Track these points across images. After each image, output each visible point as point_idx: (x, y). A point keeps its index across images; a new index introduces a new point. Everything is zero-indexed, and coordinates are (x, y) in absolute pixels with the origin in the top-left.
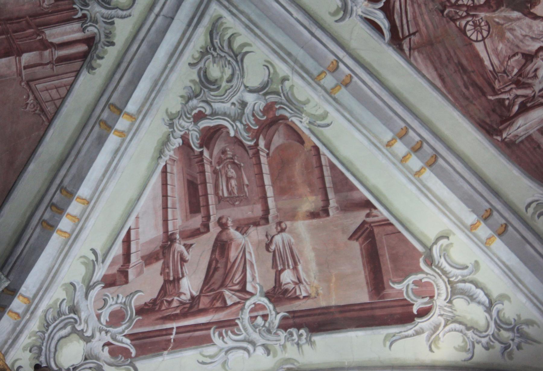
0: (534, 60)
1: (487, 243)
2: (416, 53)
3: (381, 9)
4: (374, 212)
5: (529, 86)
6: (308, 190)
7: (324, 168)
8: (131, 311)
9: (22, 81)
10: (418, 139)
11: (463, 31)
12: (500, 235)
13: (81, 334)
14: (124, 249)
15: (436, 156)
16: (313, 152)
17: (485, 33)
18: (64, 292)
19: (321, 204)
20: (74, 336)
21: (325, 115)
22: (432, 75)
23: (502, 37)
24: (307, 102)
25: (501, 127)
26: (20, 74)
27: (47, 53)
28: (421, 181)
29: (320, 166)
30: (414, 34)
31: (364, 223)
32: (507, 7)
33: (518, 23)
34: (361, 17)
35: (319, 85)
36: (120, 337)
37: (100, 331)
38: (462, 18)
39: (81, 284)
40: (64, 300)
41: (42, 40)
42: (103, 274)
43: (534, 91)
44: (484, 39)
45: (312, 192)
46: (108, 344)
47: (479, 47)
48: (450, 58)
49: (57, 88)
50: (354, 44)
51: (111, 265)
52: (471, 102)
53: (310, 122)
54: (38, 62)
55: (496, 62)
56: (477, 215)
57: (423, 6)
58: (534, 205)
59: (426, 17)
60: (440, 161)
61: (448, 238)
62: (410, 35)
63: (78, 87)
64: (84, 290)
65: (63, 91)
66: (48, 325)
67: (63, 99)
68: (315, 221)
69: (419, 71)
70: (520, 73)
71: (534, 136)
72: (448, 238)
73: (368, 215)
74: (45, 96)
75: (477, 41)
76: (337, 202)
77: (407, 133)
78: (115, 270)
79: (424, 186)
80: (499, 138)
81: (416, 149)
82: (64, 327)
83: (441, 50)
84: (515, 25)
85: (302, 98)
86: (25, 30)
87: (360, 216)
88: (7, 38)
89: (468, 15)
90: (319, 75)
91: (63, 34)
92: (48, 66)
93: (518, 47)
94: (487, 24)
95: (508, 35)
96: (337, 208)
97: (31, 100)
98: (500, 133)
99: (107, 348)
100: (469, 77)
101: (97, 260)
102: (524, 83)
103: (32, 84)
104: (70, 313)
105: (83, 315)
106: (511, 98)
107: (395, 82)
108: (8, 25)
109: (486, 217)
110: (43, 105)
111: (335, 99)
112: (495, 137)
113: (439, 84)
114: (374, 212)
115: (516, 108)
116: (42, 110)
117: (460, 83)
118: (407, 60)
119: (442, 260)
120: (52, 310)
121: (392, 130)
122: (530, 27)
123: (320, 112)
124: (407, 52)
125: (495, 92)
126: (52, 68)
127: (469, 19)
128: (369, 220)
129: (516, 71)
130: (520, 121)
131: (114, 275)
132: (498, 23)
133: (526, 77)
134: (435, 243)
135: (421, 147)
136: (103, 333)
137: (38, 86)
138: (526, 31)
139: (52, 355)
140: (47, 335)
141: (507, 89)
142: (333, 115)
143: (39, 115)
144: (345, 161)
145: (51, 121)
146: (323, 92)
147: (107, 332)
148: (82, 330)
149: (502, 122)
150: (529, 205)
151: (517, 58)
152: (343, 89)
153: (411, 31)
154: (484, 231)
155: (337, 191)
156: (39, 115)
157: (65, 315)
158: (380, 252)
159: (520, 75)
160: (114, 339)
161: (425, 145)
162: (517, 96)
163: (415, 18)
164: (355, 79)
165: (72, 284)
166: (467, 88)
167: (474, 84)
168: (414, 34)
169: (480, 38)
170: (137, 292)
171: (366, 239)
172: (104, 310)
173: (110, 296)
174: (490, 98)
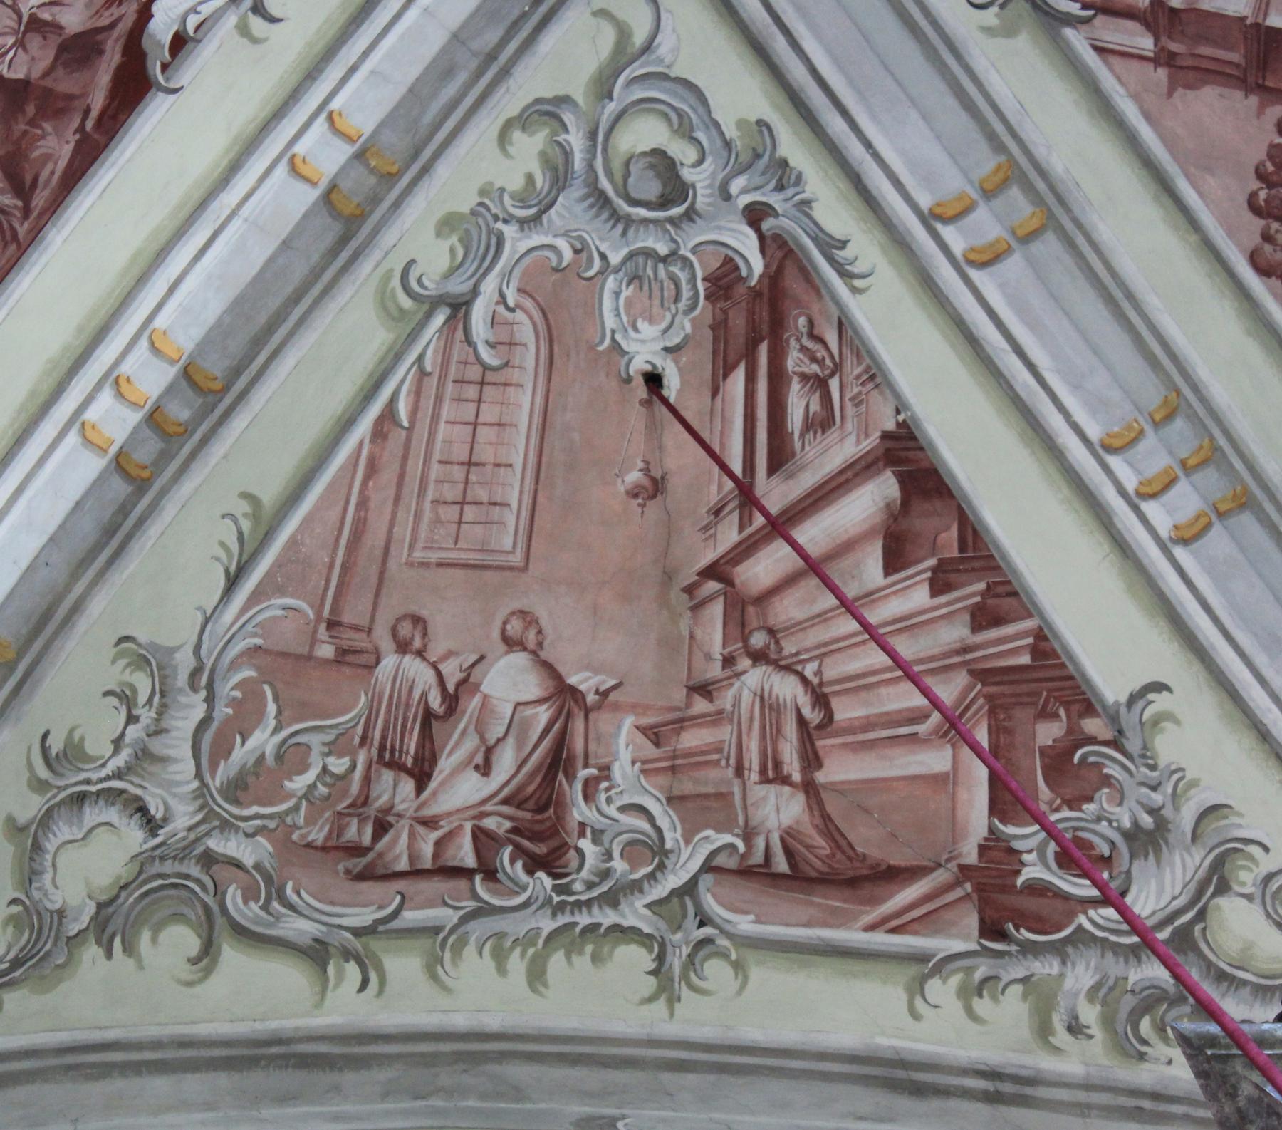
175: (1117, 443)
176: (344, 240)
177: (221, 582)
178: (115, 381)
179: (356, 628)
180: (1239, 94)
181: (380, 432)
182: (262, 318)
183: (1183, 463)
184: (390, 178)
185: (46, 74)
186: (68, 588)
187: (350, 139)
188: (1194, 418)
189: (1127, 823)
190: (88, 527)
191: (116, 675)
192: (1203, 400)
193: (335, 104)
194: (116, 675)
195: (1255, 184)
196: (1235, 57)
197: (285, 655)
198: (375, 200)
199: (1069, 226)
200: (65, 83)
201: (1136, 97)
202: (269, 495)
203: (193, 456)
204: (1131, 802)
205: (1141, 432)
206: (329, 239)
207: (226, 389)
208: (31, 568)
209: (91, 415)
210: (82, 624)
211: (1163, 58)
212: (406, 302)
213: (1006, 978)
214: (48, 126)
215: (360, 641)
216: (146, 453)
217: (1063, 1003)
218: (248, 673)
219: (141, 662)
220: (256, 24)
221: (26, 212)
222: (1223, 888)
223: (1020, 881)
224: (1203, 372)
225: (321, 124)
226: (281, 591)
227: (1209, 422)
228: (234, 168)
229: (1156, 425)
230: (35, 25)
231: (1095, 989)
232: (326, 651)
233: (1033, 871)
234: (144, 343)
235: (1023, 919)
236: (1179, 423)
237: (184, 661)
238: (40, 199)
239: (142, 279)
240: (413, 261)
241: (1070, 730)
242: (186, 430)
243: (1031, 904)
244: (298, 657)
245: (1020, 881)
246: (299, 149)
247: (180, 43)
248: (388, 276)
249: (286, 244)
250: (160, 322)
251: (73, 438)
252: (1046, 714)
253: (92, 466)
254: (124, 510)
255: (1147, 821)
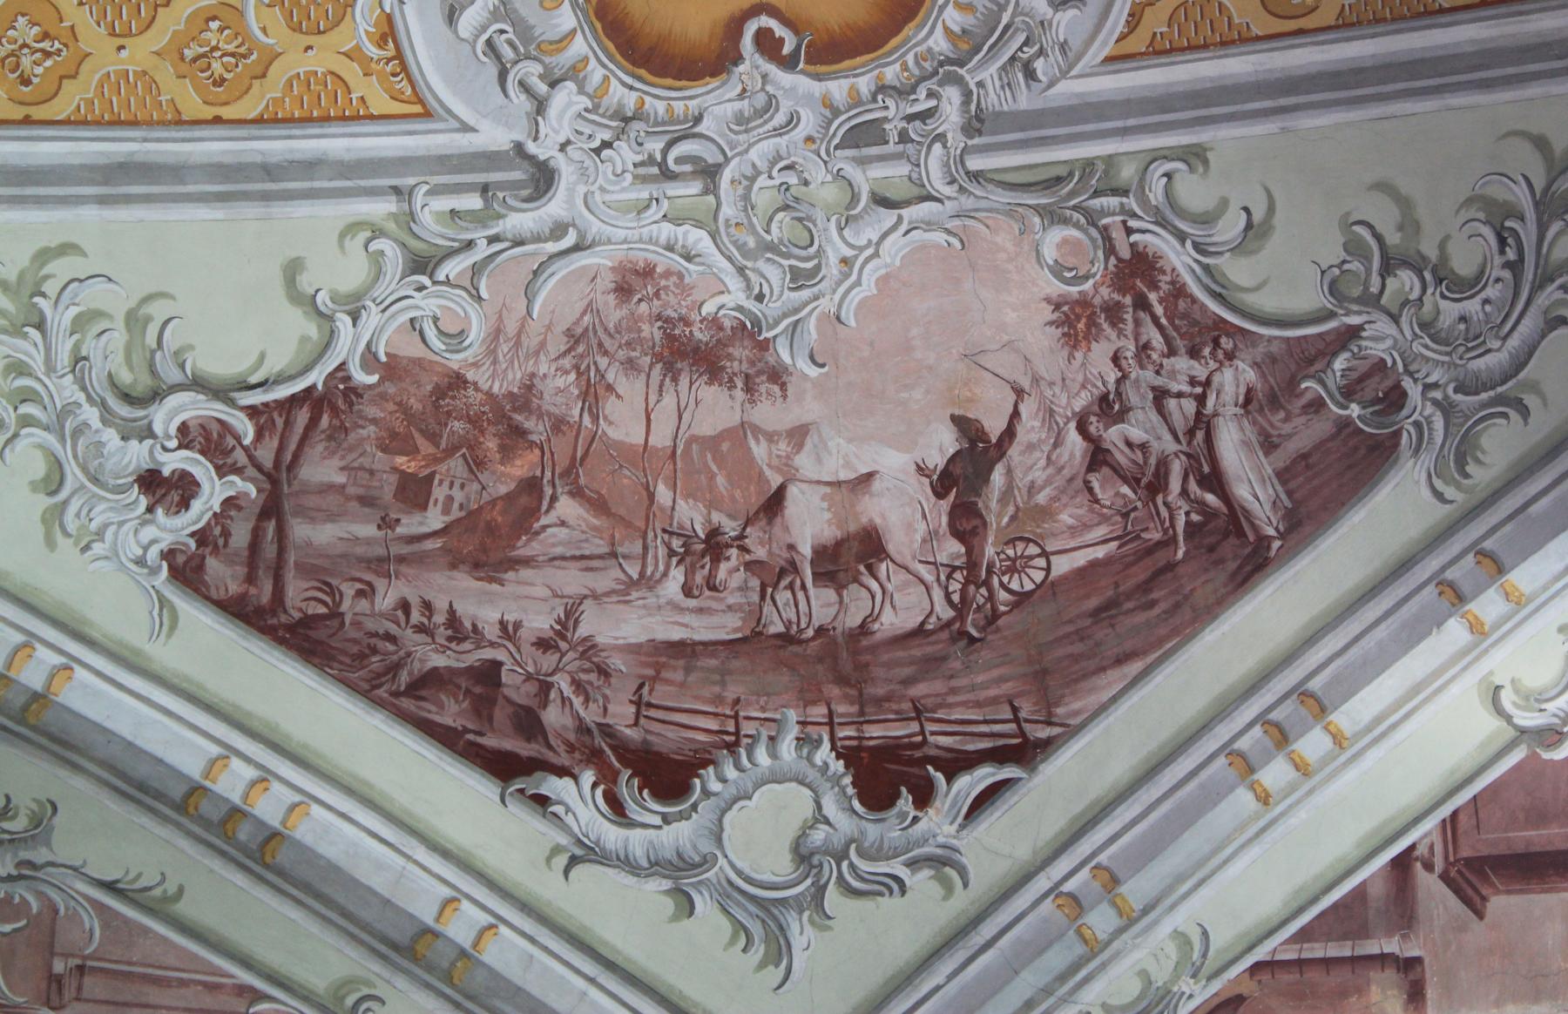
0: (1106, 446)
1: (1517, 601)
2: (1060, 711)
3: (950, 779)
4: (1422, 850)
5: (1163, 464)
6: (1353, 999)
7: (1306, 955)
10: (1257, 731)
11: (1022, 598)
12: (1501, 570)
15: (1302, 693)
16: (1265, 977)
17: (1033, 550)
19: (1390, 974)
21: (1181, 938)
22: (1114, 680)
23: (1045, 513)
24: (1144, 975)
25: (1251, 538)
28: (1358, 735)
29: (1300, 964)
30: (1015, 710)
31: (1445, 877)
32: (980, 496)
33: (1018, 474)
34: (962, 827)
35: (1108, 943)
38: (991, 597)
43: (1176, 454)
44: (1045, 554)
45: (1360, 991)
47: (1062, 565)
48: (1081, 636)
50: (1025, 852)
52: (1186, 598)
53: (1194, 976)
55: (1100, 532)
56: (1450, 616)
57: (954, 683)
58: (1439, 484)
59: (980, 679)
60: (1315, 685)
61: (1498, 688)
62: (1016, 720)
68: (1431, 993)
69: (1103, 708)
70: (1134, 482)
71: (1281, 465)
72: (1498, 688)
73: (1429, 867)
75: (1048, 570)
76: (1389, 934)
77: (1241, 755)
79: (1369, 729)
80: (1276, 544)
81: (1281, 737)
83: (1060, 652)
84: (1022, 481)
85: (1133, 988)
87: (1429, 885)
89: (987, 583)
90: (1086, 942)
93: (1071, 480)
94: (1012, 542)
95: (1041, 498)
96: (1405, 937)
98: (1263, 541)
100: (1128, 596)
102: (1157, 474)
106: (1186, 508)
107: (1119, 769)
109: (1457, 596)
111: (1146, 911)
112: (1272, 553)
113: (1135, 667)
114: (1422, 850)
115: (1210, 498)
117: (1141, 618)
118: (1072, 732)
119: (1551, 706)
121: (1232, 789)
122: (1031, 447)
123: (1172, 950)
124: (1056, 730)
125: (1169, 542)
127: (995, 581)
128: (1439, 864)
129: (1126, 490)
130: (1242, 492)
132: (1013, 518)
133: (1142, 468)
134: (1508, 719)
135: (1277, 725)
138: (1040, 458)
141: (1164, 513)
142: (1181, 918)
144: (1295, 905)
146: (1125, 936)
149: (1241, 533)
150: (1439, 496)
151: (1096, 485)
152: (1123, 889)
153: (1009, 716)
154: (1489, 605)
155: (1363, 933)
158: (1520, 848)
159: (1138, 481)
161: (1273, 716)
162: (1184, 492)
163: (978, 705)
164: (1102, 858)
166: (1152, 604)
167: (1146, 586)
168: (1015, 710)
169: (1042, 562)
171: (1485, 878)
174: (1180, 554)
176: (395, 947)
177: (108, 878)
178: (265, 777)
179: (80, 988)
181: (243, 990)
182: (327, 890)
184: (448, 978)
185: (508, 700)
186: (92, 759)
187: (475, 945)
190: (142, 770)
191: (24, 803)
193: (503, 930)
194: (24, 803)
197: (53, 933)
198: (430, 968)
200: (501, 714)
202: (183, 908)
203: (210, 845)
206: (395, 935)
207: (267, 866)
208: (105, 730)
209: (236, 763)
210: (64, 773)
212: (350, 1001)
214: (465, 704)
215: (69, 993)
216: (206, 807)
218: (35, 906)
219: (37, 821)
220: (561, 860)
221: (396, 694)
225: (486, 919)
226: (105, 926)
228: (445, 854)
230: (545, 687)
232: (59, 966)
234: (298, 798)
237: (40, 855)
238: (407, 703)
239: (349, 791)
240: (383, 1003)
242: (230, 839)
244: (52, 945)
246: (466, 905)
247: (542, 801)
248: (369, 984)
249: (387, 902)
250: (316, 810)
251: (215, 750)
253: (192, 767)
254: (159, 796)
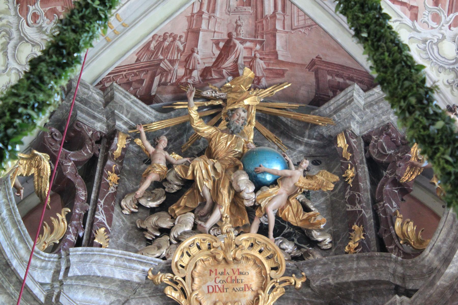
8: (435, 9)
9: (291, 32)
13: (439, 41)
14: (398, 4)
18: (413, 44)
20: (440, 45)
26: (287, 32)
27: (278, 16)
36: (448, 19)
37: (441, 29)
39: (411, 33)
40: (417, 45)
41: (271, 17)
42: (409, 19)
46: (450, 27)
49: (298, 16)
51: (405, 14)
54: (282, 22)
63: (300, 5)
64: (415, 32)
65: (301, 13)
66: (429, 58)
67: (305, 14)
74: (302, 23)
78: (408, 12)
82: (433, 49)
86: (263, 25)
88: (266, 34)
91: (269, 6)
92: (286, 17)
97: (303, 30)
99: (452, 28)
101: (400, 21)
103: (294, 28)
104: (426, 44)
105: (429, 36)
108: (259, 32)
110: (307, 25)
116: (309, 26)
120: (421, 54)
126: (287, 15)
131: (411, 14)
136: (442, 28)
137: (296, 24)
139: (446, 61)
140: (434, 61)
143: (311, 28)
145: (316, 24)
147: (443, 26)
148: (438, 39)
156: (311, 28)
157: (426, 47)
160: (448, 22)
165: (410, 38)
170: (424, 3)
172: (430, 24)
173: (423, 18)
175: (117, 17)
180: (187, 28)
183: (115, 30)
188: (124, 30)
189: (43, 26)
192: (127, 31)
195: (170, 33)
196: (194, 27)
199: (159, 3)
201: (185, 11)
204: (47, 26)
205: (120, 21)
211: (192, 15)
213: (9, 5)
217: (6, 16)
222: (33, 46)
223: (29, 6)
224: (133, 30)
227: (123, 33)
229: (122, 24)
231: (10, 22)
233: (31, 8)
235: (21, 7)
236: (122, 28)
241: (60, 13)
243: (25, 8)
245: (29, 6)
252: (63, 8)
255: (44, 29)
